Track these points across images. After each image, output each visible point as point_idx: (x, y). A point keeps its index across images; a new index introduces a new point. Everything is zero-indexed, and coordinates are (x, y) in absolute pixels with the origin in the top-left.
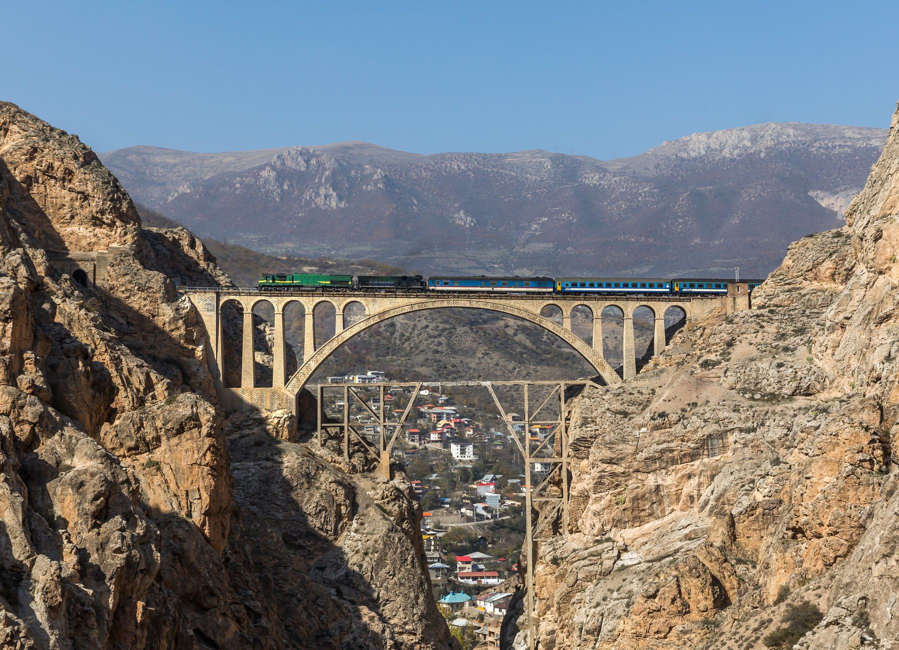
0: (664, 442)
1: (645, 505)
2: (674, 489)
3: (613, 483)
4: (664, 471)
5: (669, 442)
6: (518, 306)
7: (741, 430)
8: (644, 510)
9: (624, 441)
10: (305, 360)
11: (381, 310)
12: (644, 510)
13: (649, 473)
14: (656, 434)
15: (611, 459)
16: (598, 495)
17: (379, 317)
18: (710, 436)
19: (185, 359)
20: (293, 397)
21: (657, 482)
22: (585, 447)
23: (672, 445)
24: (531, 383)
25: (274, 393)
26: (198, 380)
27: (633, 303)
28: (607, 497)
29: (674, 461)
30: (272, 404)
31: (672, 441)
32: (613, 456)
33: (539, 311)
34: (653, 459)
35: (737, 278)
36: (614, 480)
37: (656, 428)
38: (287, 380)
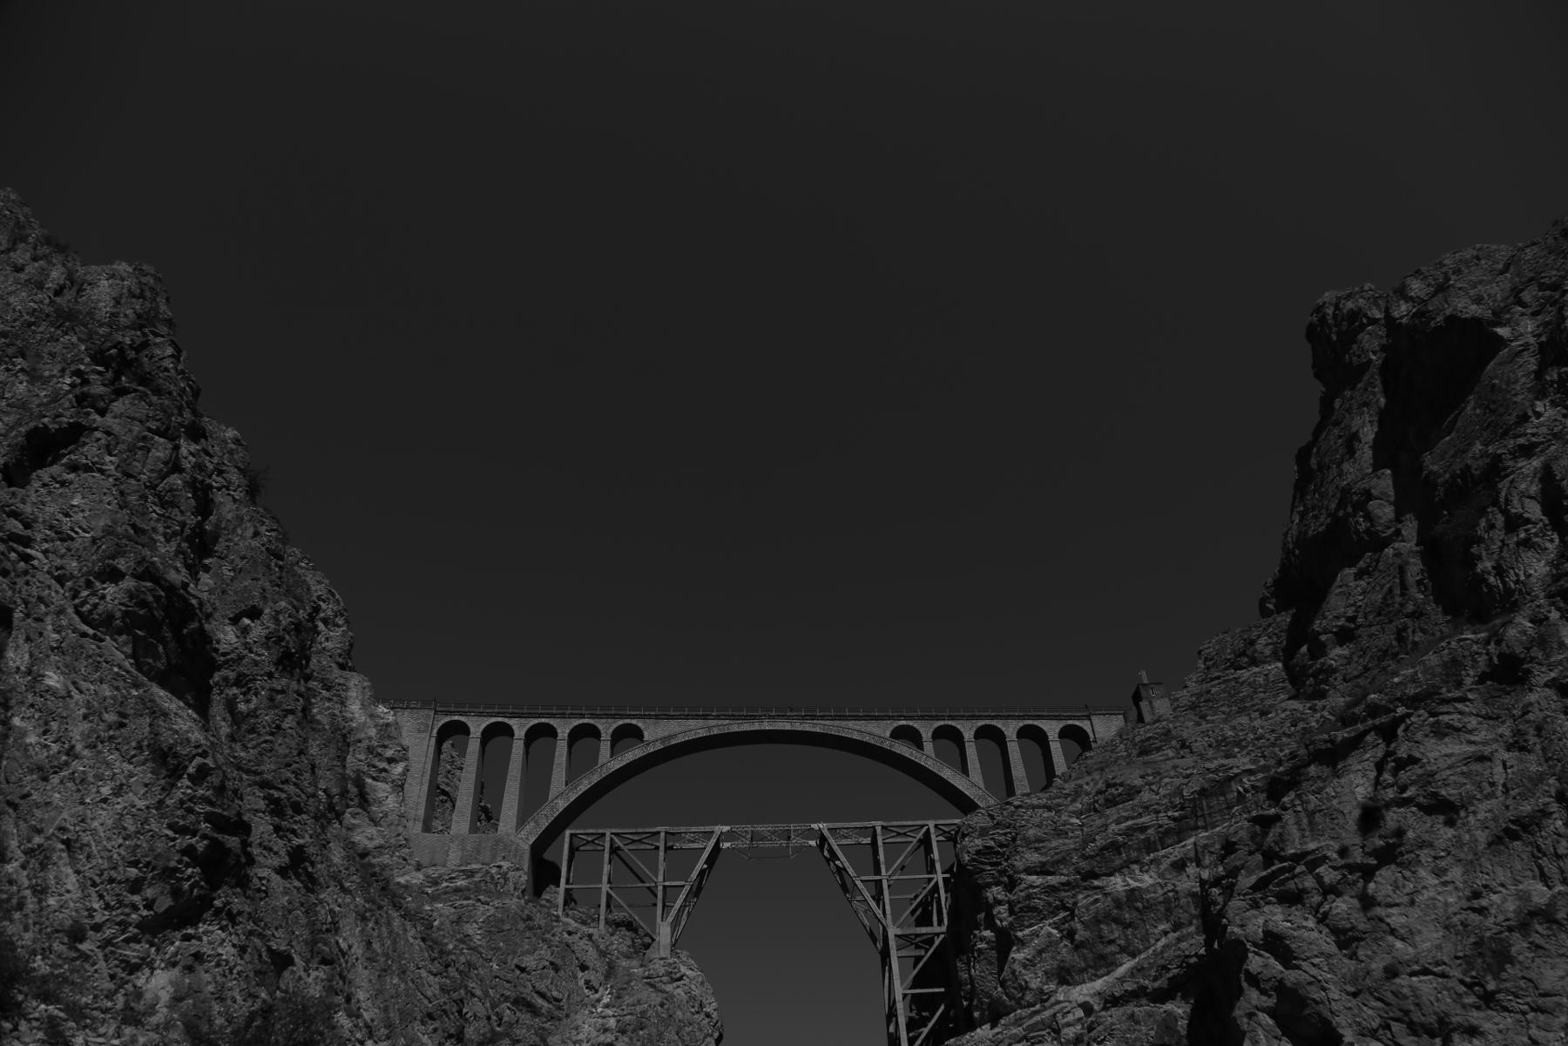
0: (1127, 819)
1: (1112, 932)
2: (1160, 892)
3: (1049, 904)
4: (1135, 867)
5: (1133, 818)
6: (858, 728)
7: (1250, 772)
8: (1111, 942)
9: (1060, 833)
10: (550, 798)
11: (666, 734)
12: (1111, 942)
13: (1111, 874)
14: (1112, 813)
15: (1043, 864)
16: (1027, 931)
17: (662, 743)
18: (1203, 792)
19: (369, 781)
20: (526, 848)
21: (1128, 885)
22: (991, 864)
23: (1143, 820)
24: (885, 824)
25: (497, 842)
26: (384, 808)
27: (1014, 722)
28: (1048, 929)
29: (1149, 847)
30: (494, 857)
31: (1140, 815)
32: (1044, 859)
33: (888, 734)
34: (1115, 847)
35: (1146, 681)
36: (1051, 899)
37: (1112, 802)
38: (522, 821)
